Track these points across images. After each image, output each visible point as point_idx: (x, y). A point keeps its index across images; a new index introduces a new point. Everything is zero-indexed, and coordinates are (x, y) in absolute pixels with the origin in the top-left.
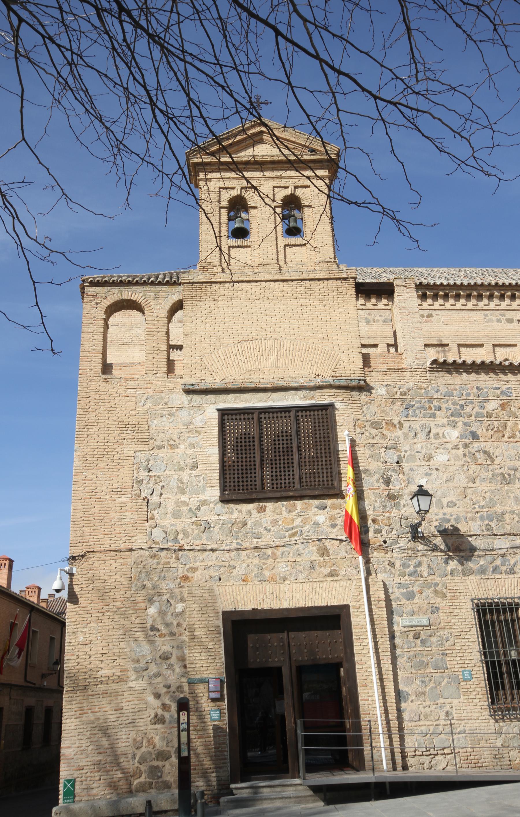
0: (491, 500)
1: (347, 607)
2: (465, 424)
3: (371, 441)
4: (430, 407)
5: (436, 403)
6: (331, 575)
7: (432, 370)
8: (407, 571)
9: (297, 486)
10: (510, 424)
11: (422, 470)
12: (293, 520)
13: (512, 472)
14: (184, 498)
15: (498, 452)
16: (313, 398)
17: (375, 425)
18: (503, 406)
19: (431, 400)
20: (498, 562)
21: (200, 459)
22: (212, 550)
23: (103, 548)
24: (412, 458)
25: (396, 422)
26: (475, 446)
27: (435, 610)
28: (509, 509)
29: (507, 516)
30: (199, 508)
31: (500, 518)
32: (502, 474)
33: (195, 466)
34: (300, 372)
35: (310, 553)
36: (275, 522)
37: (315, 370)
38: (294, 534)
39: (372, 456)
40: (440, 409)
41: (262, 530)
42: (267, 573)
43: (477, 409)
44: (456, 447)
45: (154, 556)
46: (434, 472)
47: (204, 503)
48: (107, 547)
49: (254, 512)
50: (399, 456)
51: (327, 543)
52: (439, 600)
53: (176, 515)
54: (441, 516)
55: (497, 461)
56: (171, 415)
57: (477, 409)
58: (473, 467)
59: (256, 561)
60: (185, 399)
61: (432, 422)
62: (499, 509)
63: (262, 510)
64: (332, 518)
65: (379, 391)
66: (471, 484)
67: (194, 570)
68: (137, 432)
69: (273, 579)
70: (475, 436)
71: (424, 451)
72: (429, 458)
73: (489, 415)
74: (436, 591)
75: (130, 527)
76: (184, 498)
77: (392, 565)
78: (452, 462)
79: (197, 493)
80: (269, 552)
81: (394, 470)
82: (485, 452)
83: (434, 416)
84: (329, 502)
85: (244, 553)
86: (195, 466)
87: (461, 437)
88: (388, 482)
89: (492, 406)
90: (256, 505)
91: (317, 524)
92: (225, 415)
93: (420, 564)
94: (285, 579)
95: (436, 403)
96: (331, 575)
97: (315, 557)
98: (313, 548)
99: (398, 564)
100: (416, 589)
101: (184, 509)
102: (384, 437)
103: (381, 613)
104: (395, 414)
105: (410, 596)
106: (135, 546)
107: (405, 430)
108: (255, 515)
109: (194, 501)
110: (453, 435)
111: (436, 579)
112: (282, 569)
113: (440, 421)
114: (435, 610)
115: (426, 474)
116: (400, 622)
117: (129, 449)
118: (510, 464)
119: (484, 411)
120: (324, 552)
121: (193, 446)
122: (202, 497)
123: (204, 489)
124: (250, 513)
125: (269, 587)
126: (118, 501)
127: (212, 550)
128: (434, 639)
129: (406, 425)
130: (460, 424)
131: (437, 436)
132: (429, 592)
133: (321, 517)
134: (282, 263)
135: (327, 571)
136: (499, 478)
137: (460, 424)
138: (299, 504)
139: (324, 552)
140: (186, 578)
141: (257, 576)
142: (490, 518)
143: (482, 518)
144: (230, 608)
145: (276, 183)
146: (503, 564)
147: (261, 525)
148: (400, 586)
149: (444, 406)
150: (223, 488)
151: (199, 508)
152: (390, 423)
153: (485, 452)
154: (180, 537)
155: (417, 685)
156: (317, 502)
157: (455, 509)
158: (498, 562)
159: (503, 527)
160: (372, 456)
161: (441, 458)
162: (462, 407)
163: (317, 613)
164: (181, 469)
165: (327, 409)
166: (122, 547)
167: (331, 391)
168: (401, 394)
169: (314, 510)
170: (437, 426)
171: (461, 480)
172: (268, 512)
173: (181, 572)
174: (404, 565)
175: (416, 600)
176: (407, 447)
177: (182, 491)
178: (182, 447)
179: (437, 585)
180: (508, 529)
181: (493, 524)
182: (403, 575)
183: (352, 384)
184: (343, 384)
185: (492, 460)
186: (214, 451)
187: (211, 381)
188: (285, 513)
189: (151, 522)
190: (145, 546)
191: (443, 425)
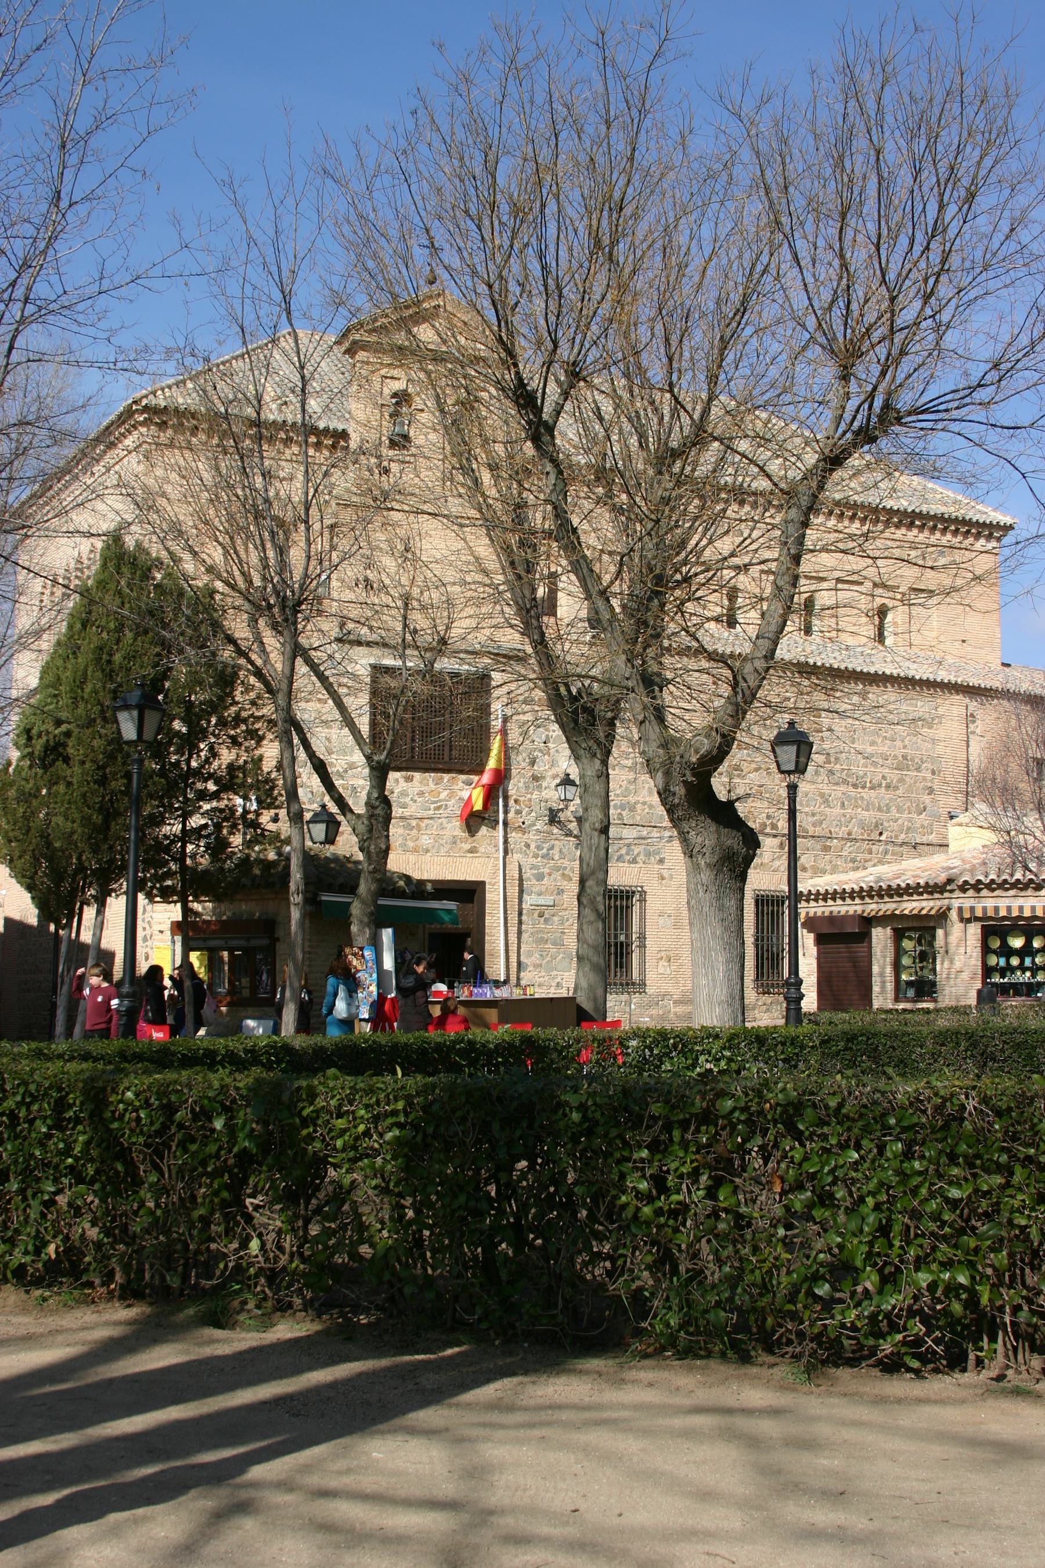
0: (627, 789)
1: (483, 883)
6: (471, 851)
9: (446, 758)
29: (639, 807)
30: (346, 771)
31: (632, 808)
36: (421, 794)
38: (438, 808)
41: (408, 800)
42: (410, 844)
49: (402, 781)
62: (632, 799)
63: (409, 779)
69: (415, 850)
77: (528, 846)
79: (345, 754)
80: (414, 823)
81: (540, 751)
88: (533, 763)
90: (404, 773)
93: (552, 848)
94: (427, 851)
96: (471, 851)
99: (533, 846)
100: (546, 870)
103: (513, 891)
105: (540, 877)
112: (426, 841)
116: (529, 900)
125: (412, 858)
128: (556, 919)
132: (557, 875)
135: (467, 846)
138: (446, 777)
141: (401, 845)
146: (627, 854)
148: (533, 867)
151: (346, 771)
155: (535, 958)
158: (623, 851)
159: (633, 817)
163: (455, 887)
165: (484, 678)
169: (461, 784)
174: (539, 848)
181: (624, 813)
182: (536, 856)
188: (432, 786)
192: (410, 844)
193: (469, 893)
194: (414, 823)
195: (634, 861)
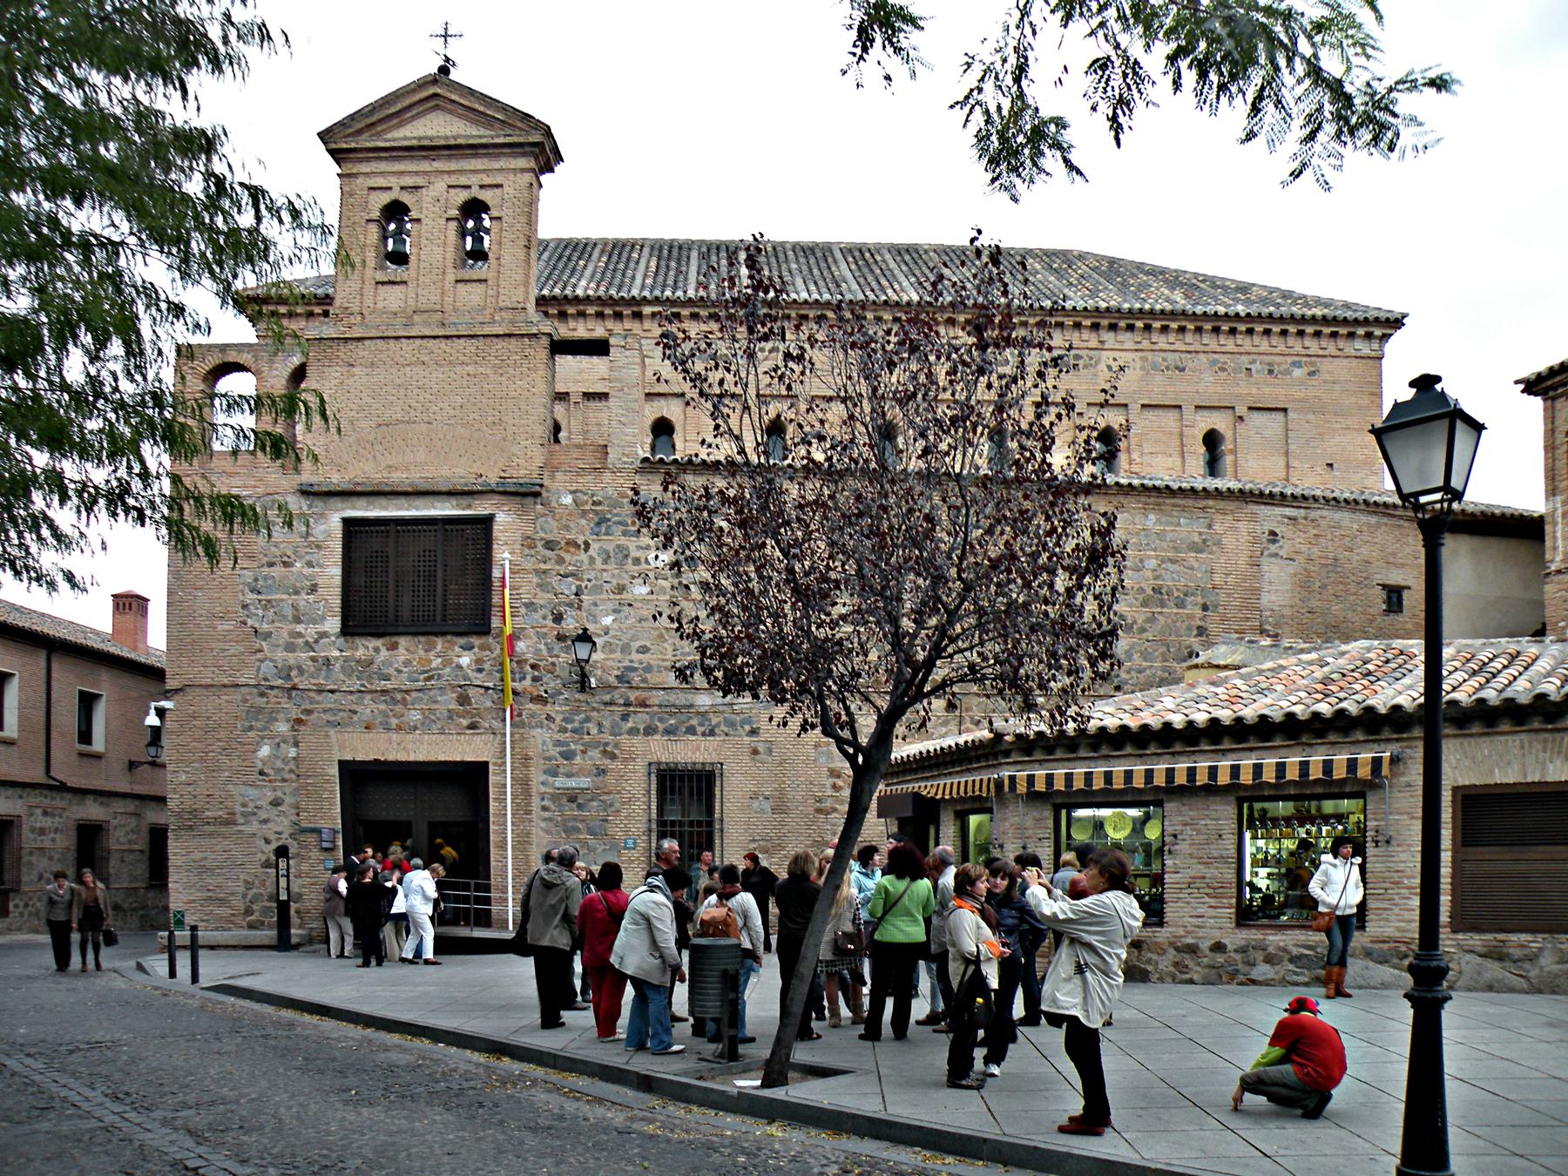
3: (543, 566)
6: (472, 726)
8: (569, 726)
9: (438, 619)
11: (611, 606)
12: (430, 661)
14: (300, 628)
16: (469, 507)
17: (549, 545)
22: (332, 691)
23: (204, 682)
24: (598, 589)
25: (580, 542)
35: (449, 701)
36: (407, 663)
37: (477, 468)
38: (429, 678)
39: (540, 585)
41: (391, 671)
42: (394, 722)
45: (262, 695)
46: (627, 609)
47: (324, 635)
48: (209, 681)
49: (383, 649)
50: (579, 587)
51: (471, 692)
52: (608, 762)
53: (290, 648)
54: (627, 664)
59: (383, 707)
61: (631, 544)
64: (478, 661)
67: (309, 712)
71: (614, 582)
72: (621, 589)
74: (605, 752)
75: (235, 660)
76: (300, 628)
80: (399, 696)
81: (570, 605)
84: (476, 641)
85: (369, 697)
86: (313, 589)
88: (558, 618)
91: (459, 667)
94: (415, 728)
96: (472, 726)
99: (559, 718)
100: (580, 747)
102: (561, 561)
104: (581, 529)
106: (242, 681)
107: (592, 552)
108: (384, 653)
109: (310, 632)
112: (415, 716)
114: (602, 772)
115: (615, 611)
120: (464, 700)
122: (320, 628)
123: (323, 618)
124: (377, 650)
127: (332, 691)
129: (594, 546)
131: (637, 561)
132: (595, 753)
135: (465, 722)
139: (464, 700)
140: (299, 721)
144: (349, 757)
147: (391, 664)
151: (316, 641)
154: (294, 673)
156: (462, 641)
160: (540, 585)
166: (226, 681)
167: (496, 499)
168: (594, 503)
169: (457, 649)
170: (639, 548)
172: (401, 650)
173: (295, 713)
175: (578, 760)
179: (606, 744)
182: (563, 730)
183: (522, 490)
184: (512, 489)
188: (422, 653)
189: (259, 655)
190: (252, 682)
192: (394, 722)
193: (472, 777)
194: (399, 696)
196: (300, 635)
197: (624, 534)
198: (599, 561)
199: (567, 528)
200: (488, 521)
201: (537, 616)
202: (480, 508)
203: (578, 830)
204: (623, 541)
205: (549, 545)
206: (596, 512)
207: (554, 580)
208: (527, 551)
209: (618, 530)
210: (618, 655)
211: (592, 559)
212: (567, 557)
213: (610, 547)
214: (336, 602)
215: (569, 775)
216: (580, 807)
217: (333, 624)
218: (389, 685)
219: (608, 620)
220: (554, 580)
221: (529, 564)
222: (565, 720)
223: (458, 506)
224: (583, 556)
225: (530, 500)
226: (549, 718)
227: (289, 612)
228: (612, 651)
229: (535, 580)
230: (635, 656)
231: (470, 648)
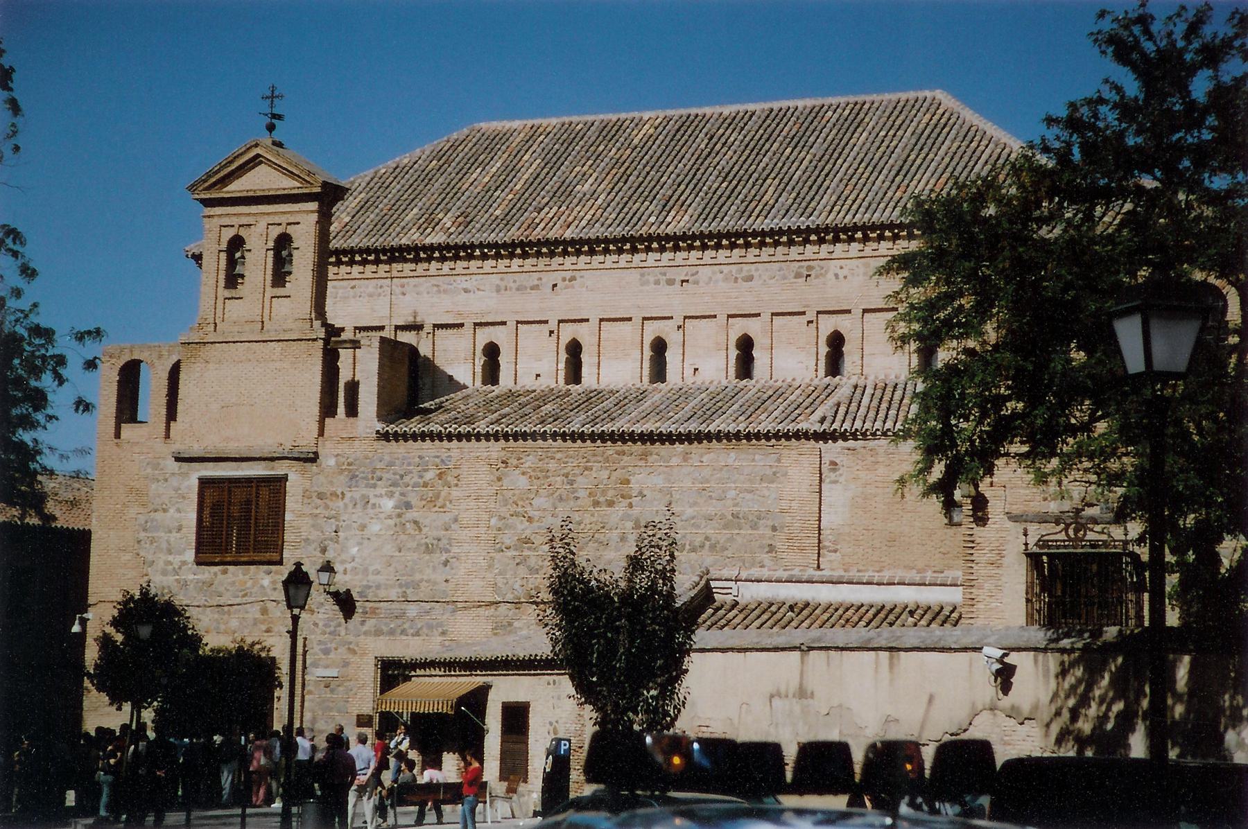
2: (402, 494)
4: (374, 478)
5: (378, 473)
7: (378, 439)
10: (443, 494)
13: (435, 542)
14: (170, 558)
15: (427, 522)
16: (273, 469)
17: (321, 496)
18: (440, 476)
19: (374, 471)
20: (406, 626)
21: (184, 523)
24: (349, 527)
25: (339, 493)
26: (410, 515)
27: (346, 664)
28: (425, 578)
32: (427, 544)
33: (179, 529)
34: (266, 443)
39: (313, 526)
40: (380, 479)
42: (222, 627)
43: (416, 479)
44: (390, 517)
46: (366, 542)
47: (184, 563)
51: (270, 605)
53: (164, 573)
54: (365, 583)
55: (425, 530)
56: (166, 480)
57: (416, 479)
58: (403, 537)
59: (216, 616)
60: (174, 466)
61: (371, 493)
62: (418, 577)
63: (225, 572)
64: (274, 582)
65: (328, 461)
66: (397, 554)
68: (138, 494)
70: (408, 506)
71: (360, 521)
72: (363, 527)
73: (425, 485)
76: (170, 558)
78: (383, 532)
81: (331, 540)
82: (416, 522)
83: (374, 486)
87: (396, 507)
88: (324, 550)
89: (429, 475)
91: (262, 587)
92: (205, 483)
95: (378, 473)
97: (258, 615)
98: (257, 607)
99: (321, 624)
100: (333, 645)
101: (170, 567)
102: (327, 507)
105: (326, 652)
107: (347, 500)
108: (220, 576)
110: (388, 504)
111: (351, 638)
113: (379, 491)
117: (132, 512)
118: (435, 533)
119: (421, 481)
120: (264, 611)
121: (179, 511)
122: (182, 558)
126: (123, 558)
128: (341, 689)
129: (348, 495)
130: (397, 494)
132: (342, 650)
133: (266, 582)
134: (266, 319)
135: (264, 627)
136: (423, 548)
137: (397, 494)
139: (264, 611)
142: (407, 585)
143: (401, 586)
145: (271, 220)
149: (385, 476)
150: (198, 551)
152: (334, 494)
153: (416, 522)
157: (378, 577)
158: (406, 626)
160: (313, 526)
161: (375, 527)
162: (402, 477)
164: (170, 532)
168: (349, 464)
171: (389, 549)
172: (229, 575)
175: (332, 656)
176: (345, 517)
177: (170, 552)
178: (172, 511)
180: (422, 597)
183: (302, 456)
185: (420, 530)
186: (193, 516)
187: (196, 450)
188: (241, 576)
191: (381, 496)
192: (222, 627)
195: (417, 634)
196: (170, 563)
197: (366, 486)
198: (351, 506)
199: (331, 483)
200: (284, 478)
201: (311, 548)
202: (279, 469)
203: (331, 709)
204: (365, 491)
205: (321, 496)
206: (350, 471)
207: (321, 521)
208: (306, 501)
209: (362, 483)
210: (360, 576)
211: (346, 505)
212: (330, 504)
213: (357, 496)
214: (193, 537)
215: (326, 667)
216: (332, 691)
217: (190, 555)
218: (222, 601)
219: (354, 550)
220: (321, 521)
221: (307, 510)
222: (325, 625)
223: (266, 468)
224: (341, 504)
225: (308, 465)
226: (316, 624)
227: (164, 545)
228: (357, 574)
229: (311, 522)
230: (371, 577)
231: (269, 573)
